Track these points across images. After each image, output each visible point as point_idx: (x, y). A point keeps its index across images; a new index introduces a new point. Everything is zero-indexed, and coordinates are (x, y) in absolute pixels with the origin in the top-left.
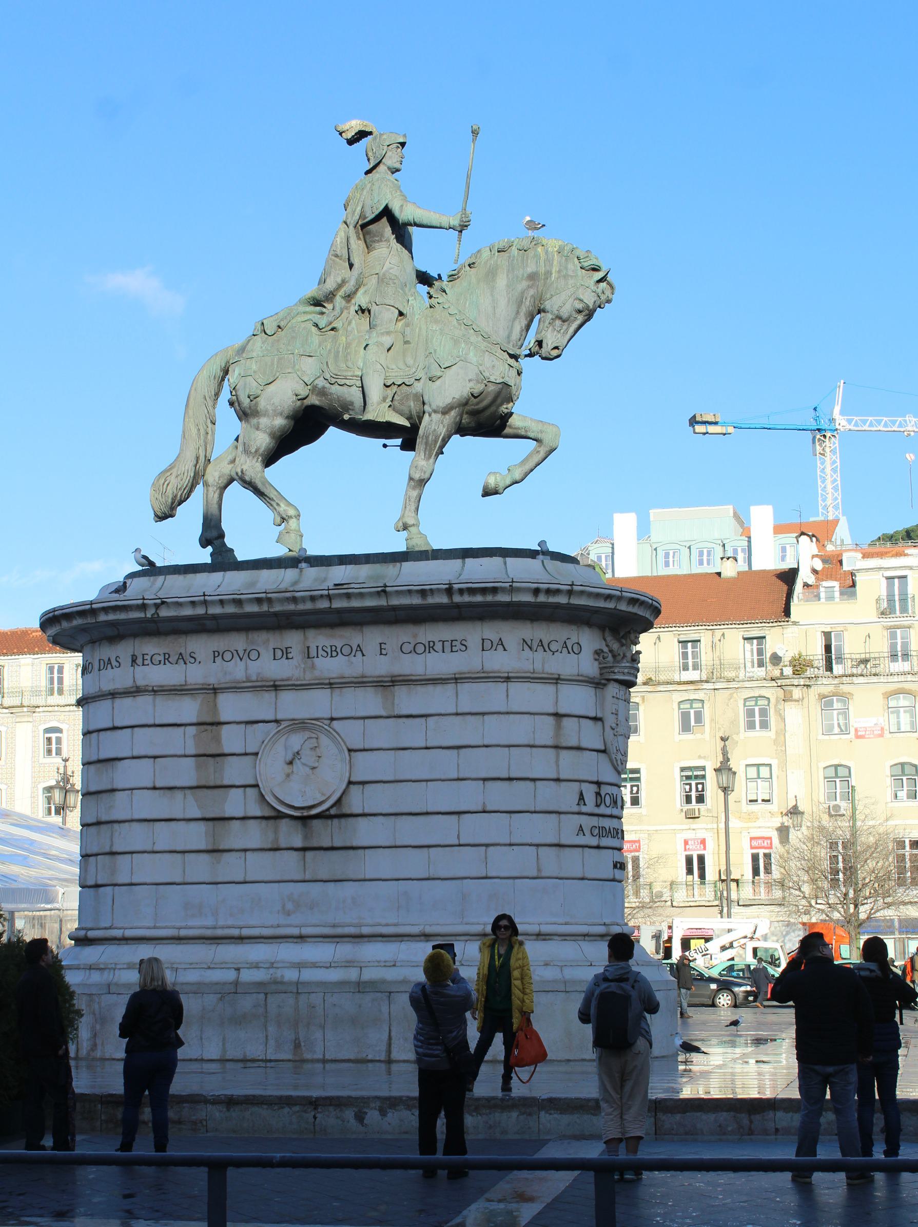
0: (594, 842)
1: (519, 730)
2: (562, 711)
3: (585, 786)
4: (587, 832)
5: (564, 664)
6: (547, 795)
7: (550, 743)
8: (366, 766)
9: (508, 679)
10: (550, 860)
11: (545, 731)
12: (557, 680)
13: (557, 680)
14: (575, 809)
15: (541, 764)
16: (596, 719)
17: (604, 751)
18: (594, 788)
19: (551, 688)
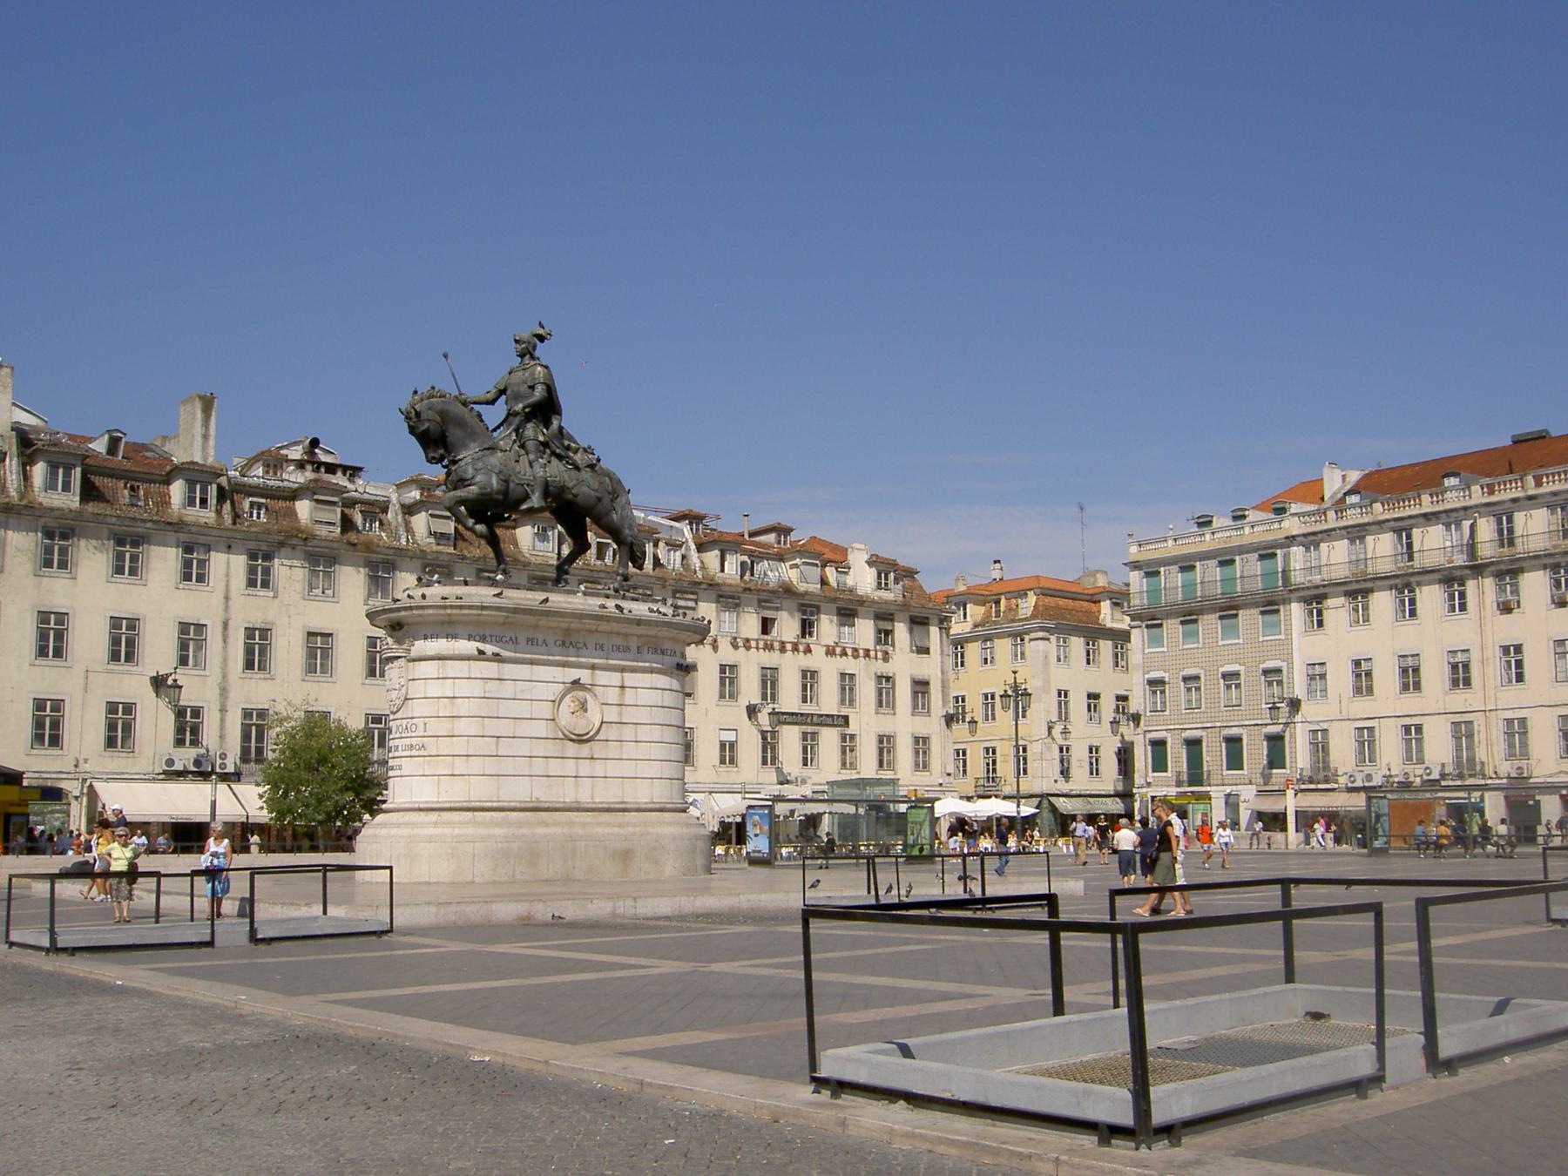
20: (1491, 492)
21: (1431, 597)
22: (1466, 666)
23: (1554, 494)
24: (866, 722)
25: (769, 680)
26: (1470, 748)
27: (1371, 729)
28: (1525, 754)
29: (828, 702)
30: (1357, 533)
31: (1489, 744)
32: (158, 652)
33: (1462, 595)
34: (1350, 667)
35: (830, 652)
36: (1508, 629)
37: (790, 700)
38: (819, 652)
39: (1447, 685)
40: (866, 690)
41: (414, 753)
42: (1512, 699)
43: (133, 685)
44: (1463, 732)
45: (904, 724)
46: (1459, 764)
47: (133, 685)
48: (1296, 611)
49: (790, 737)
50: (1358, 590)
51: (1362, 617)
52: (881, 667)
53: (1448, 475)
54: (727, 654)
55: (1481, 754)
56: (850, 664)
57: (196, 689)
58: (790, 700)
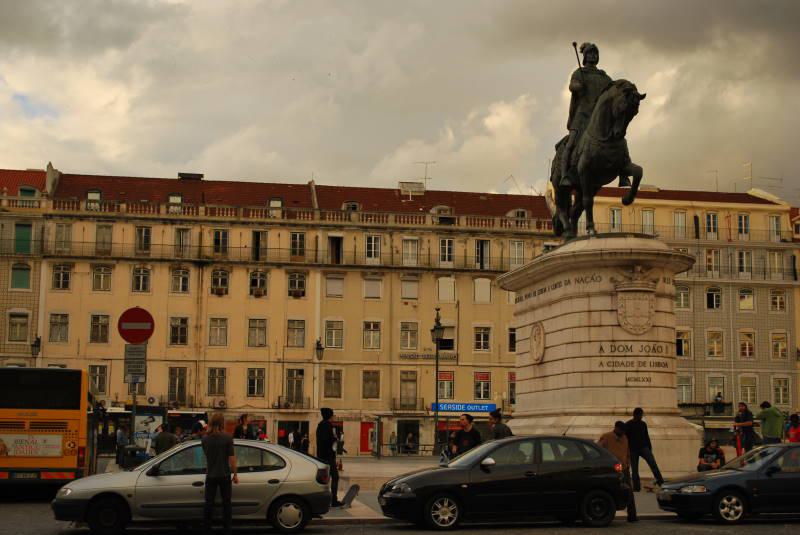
0: (610, 369)
1: (574, 320)
2: (592, 308)
3: (603, 344)
4: (605, 364)
5: (593, 287)
6: (587, 349)
7: (587, 324)
8: (551, 340)
9: (571, 298)
10: (588, 379)
11: (583, 319)
12: (588, 295)
13: (588, 295)
14: (598, 354)
15: (582, 335)
16: (612, 311)
17: (619, 325)
18: (609, 344)
19: (586, 300)
20: (213, 213)
21: (161, 277)
22: (184, 331)
23: (261, 224)
26: (182, 387)
27: (103, 369)
28: (222, 391)
31: (198, 384)
33: (185, 280)
34: (89, 321)
36: (216, 306)
39: (169, 340)
41: (661, 369)
42: (215, 356)
44: (177, 375)
46: (172, 396)
48: (45, 273)
50: (102, 261)
53: (173, 195)
55: (190, 390)
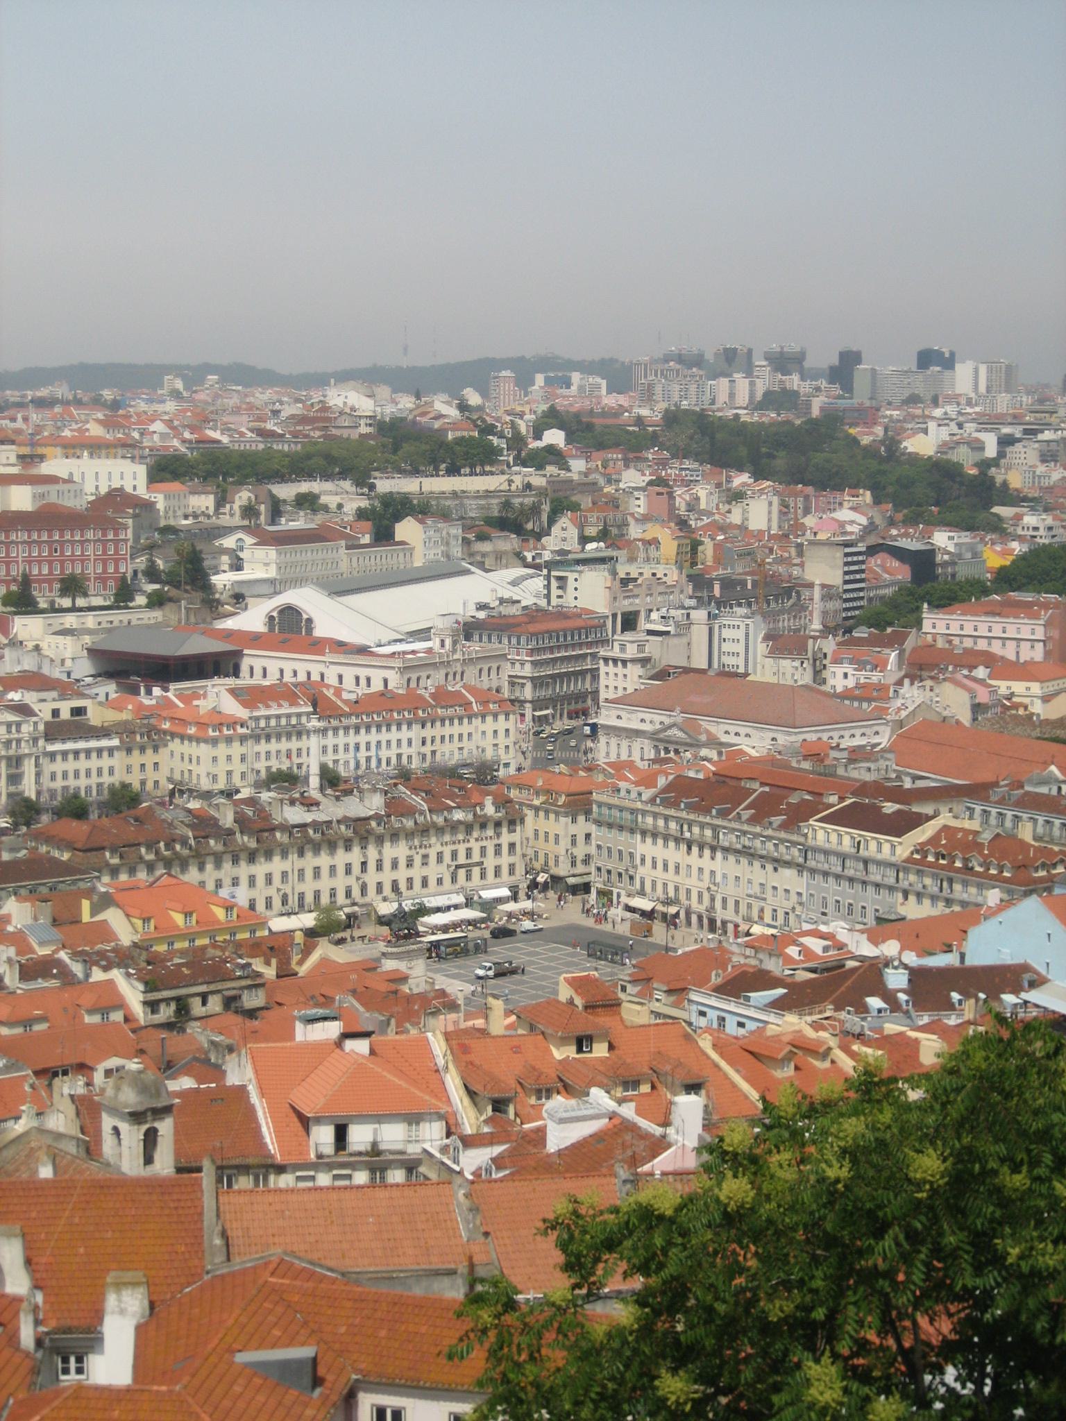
24: (490, 862)
25: (454, 855)
29: (476, 857)
30: (655, 815)
32: (277, 879)
35: (477, 840)
37: (462, 859)
38: (472, 841)
40: (490, 851)
43: (272, 891)
45: (505, 860)
47: (272, 891)
49: (462, 873)
51: (654, 843)
52: (496, 841)
54: (439, 848)
56: (484, 843)
57: (287, 889)
58: (462, 859)
